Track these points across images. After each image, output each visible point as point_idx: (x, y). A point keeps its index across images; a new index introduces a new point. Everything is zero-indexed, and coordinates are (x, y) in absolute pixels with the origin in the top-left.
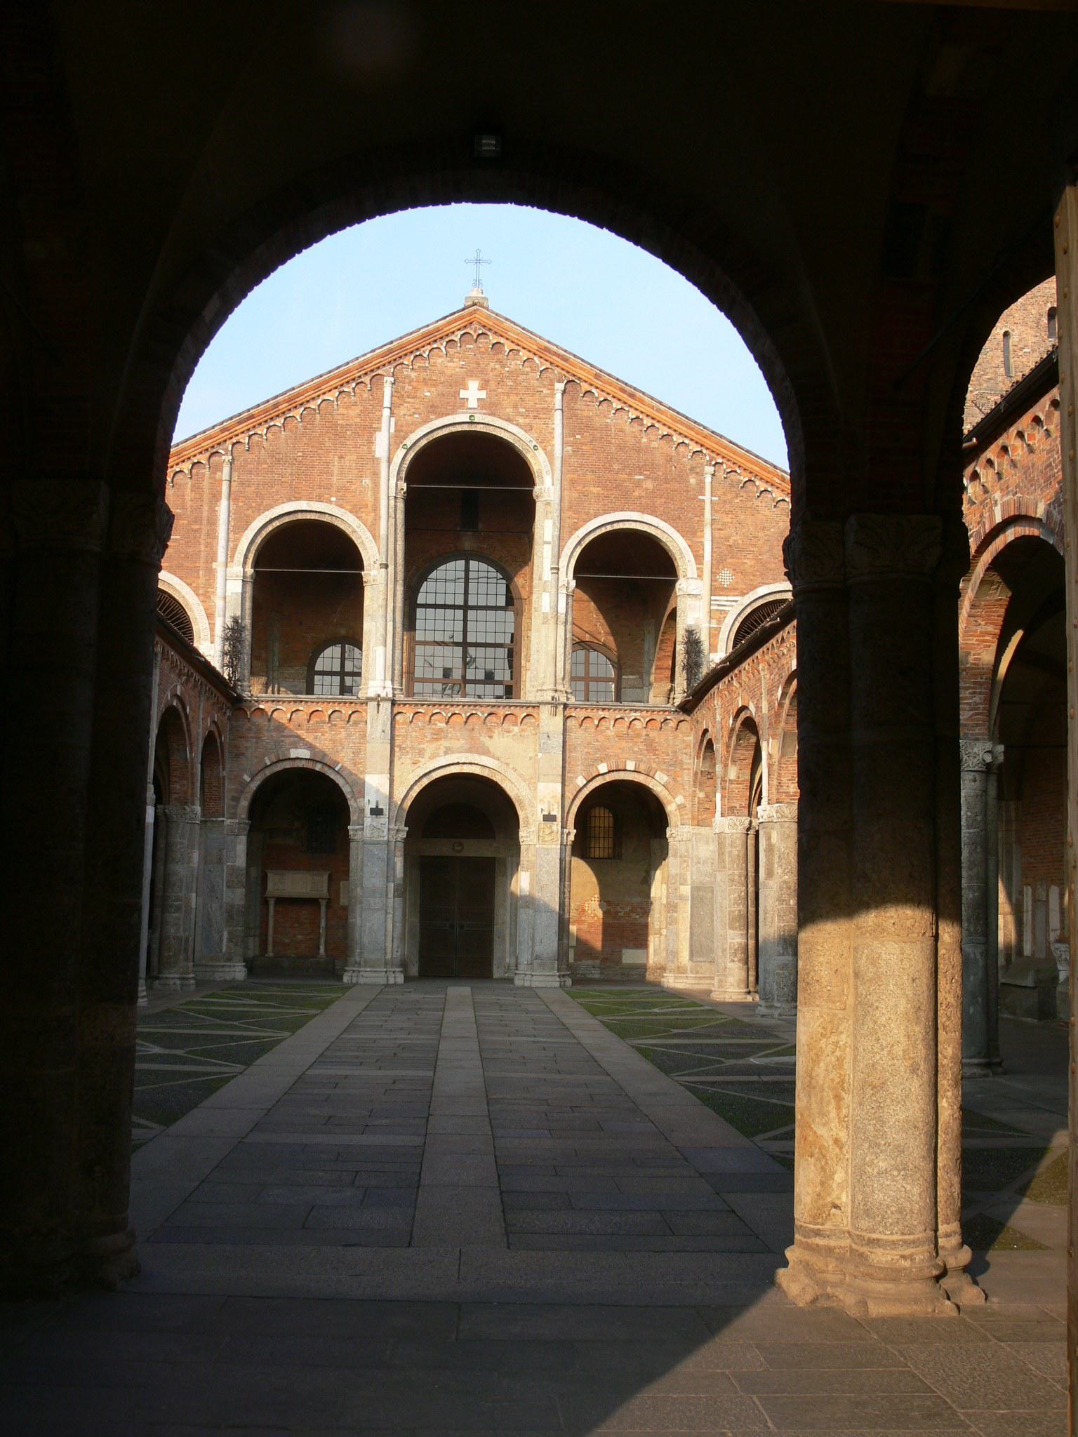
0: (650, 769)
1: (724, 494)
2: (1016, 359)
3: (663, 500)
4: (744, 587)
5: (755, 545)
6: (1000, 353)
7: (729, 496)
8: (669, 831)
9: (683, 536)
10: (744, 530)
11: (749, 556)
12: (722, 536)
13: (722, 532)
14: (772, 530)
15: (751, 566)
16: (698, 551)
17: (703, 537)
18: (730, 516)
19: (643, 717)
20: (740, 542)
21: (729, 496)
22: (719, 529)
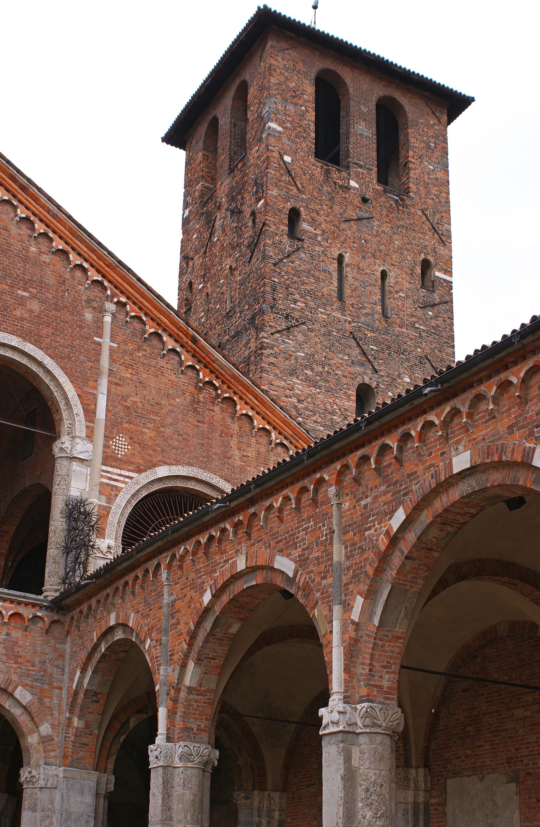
0: (9, 681)
1: (125, 342)
2: (392, 300)
3: (51, 331)
4: (142, 462)
5: (157, 414)
6: (377, 290)
7: (130, 347)
8: (24, 774)
9: (72, 382)
10: (145, 392)
11: (149, 425)
12: (119, 392)
13: (119, 388)
14: (178, 400)
15: (151, 437)
16: (89, 405)
17: (96, 388)
18: (130, 370)
19: (5, 608)
20: (140, 405)
21: (130, 347)
22: (116, 384)
